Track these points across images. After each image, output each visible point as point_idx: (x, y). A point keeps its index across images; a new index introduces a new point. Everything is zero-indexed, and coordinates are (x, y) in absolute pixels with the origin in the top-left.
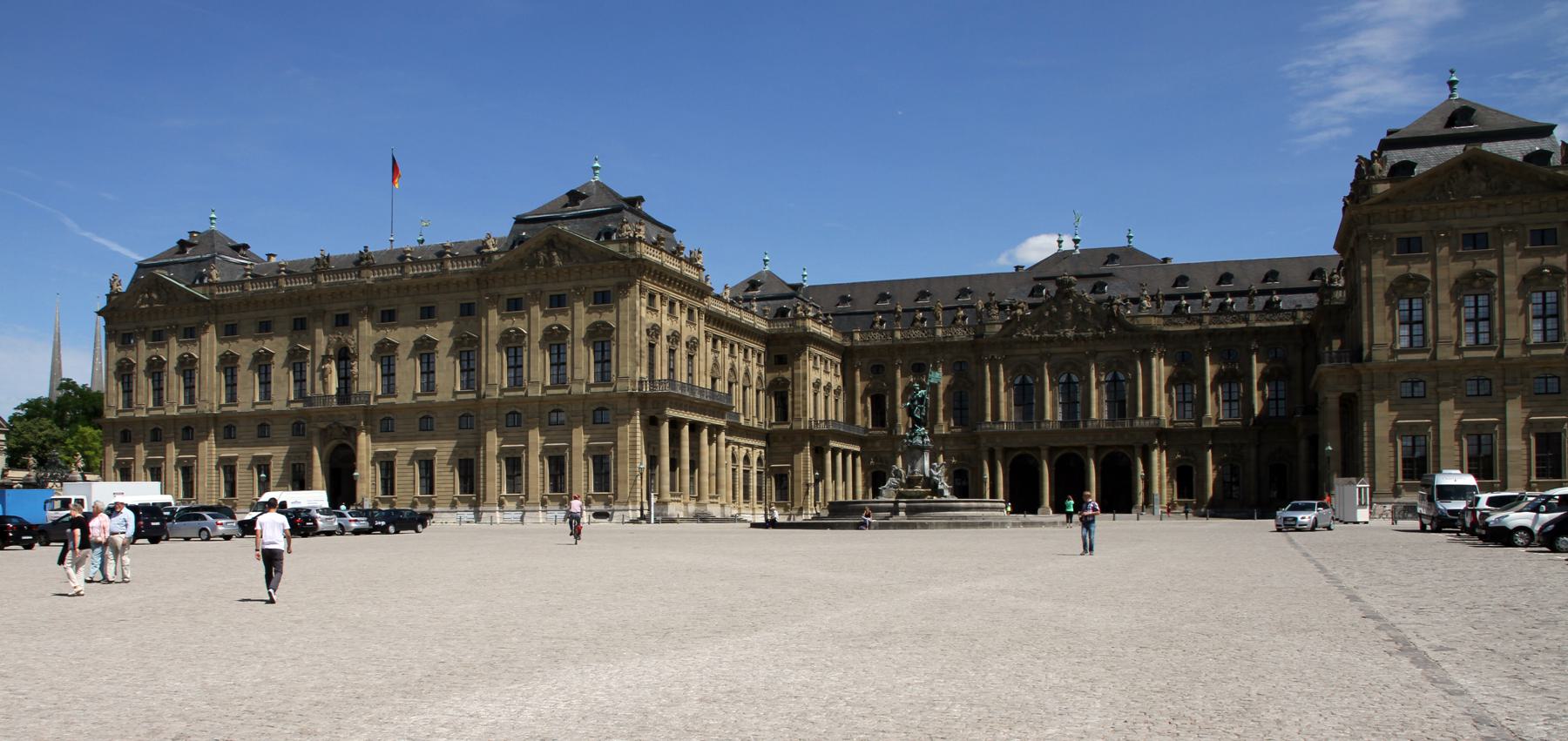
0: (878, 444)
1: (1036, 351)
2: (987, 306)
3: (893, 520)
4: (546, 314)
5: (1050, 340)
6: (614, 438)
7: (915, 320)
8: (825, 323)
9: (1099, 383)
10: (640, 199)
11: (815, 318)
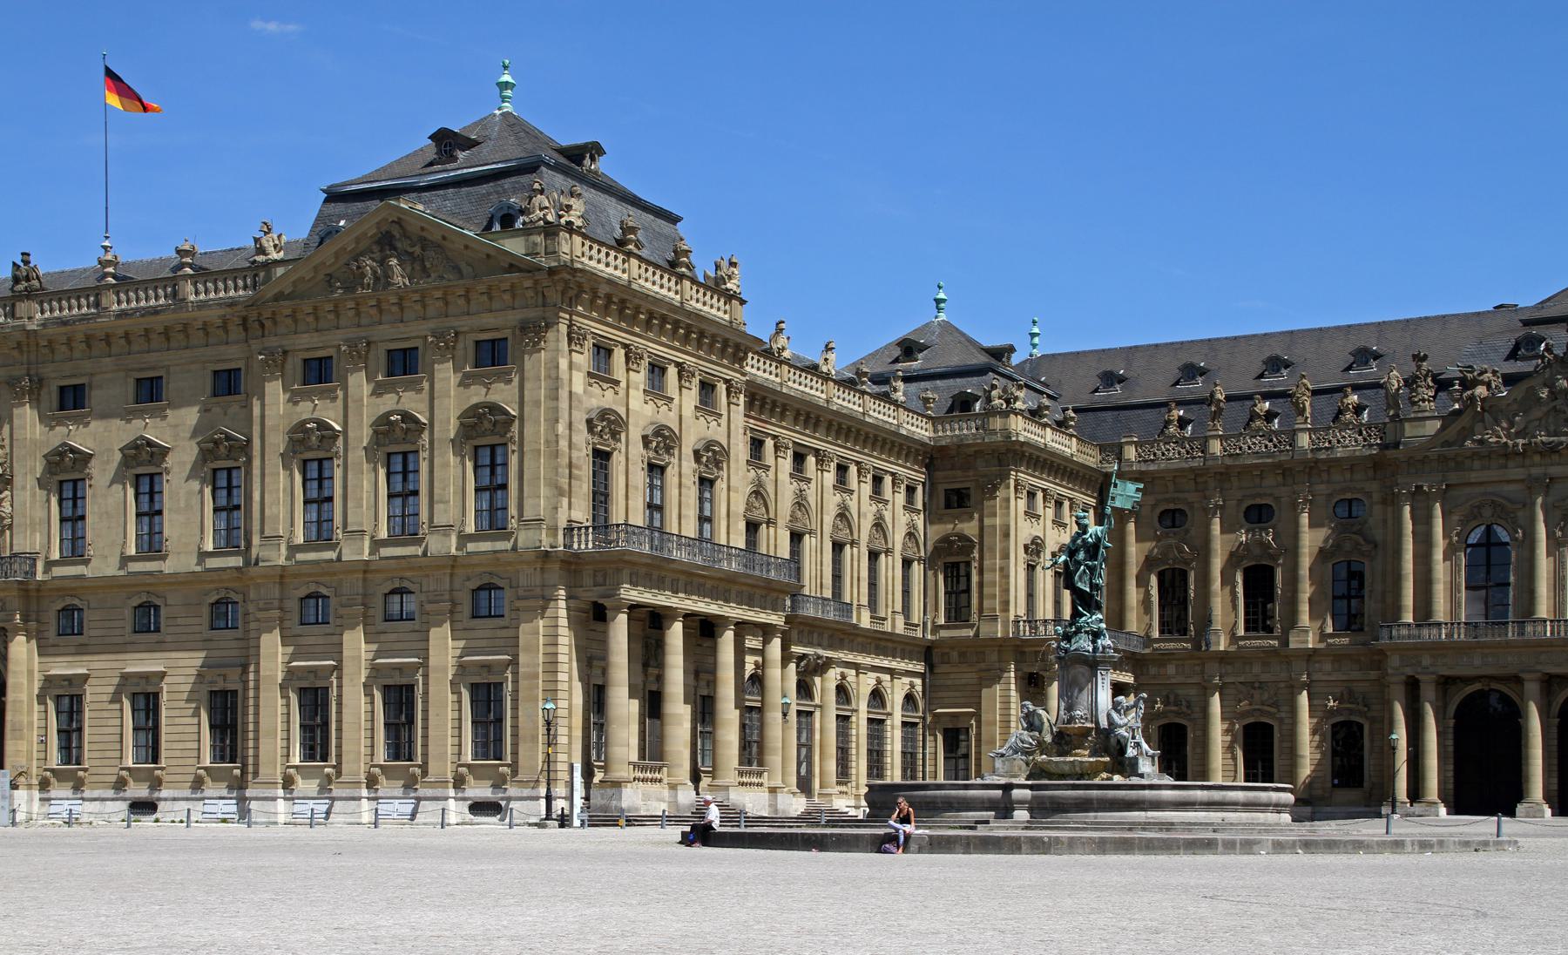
0: (1171, 669)
1: (1515, 472)
2: (1410, 382)
3: (999, 829)
4: (377, 392)
6: (513, 646)
7: (1253, 416)
8: (1061, 425)
10: (595, 150)
11: (1034, 414)
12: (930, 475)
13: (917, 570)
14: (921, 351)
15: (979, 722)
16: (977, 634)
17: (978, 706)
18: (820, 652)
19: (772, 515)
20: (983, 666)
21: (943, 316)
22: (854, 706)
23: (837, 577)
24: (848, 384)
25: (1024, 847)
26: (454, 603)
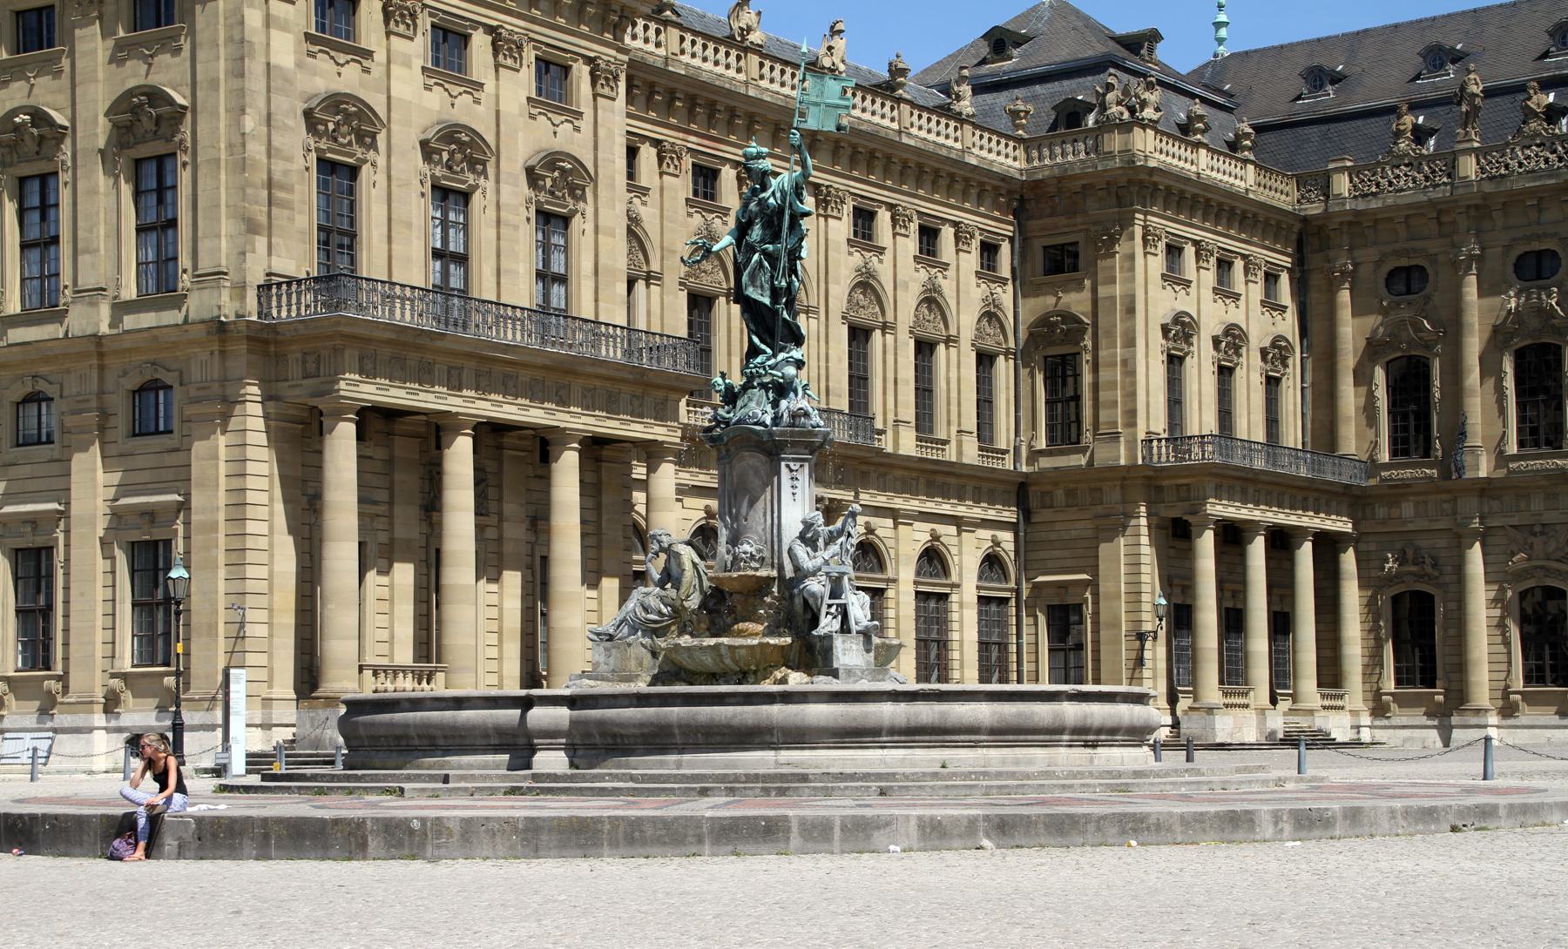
0: (1407, 509)
6: (181, 479)
12: (1021, 227)
13: (1003, 369)
14: (1018, 45)
15: (1096, 595)
16: (1091, 463)
17: (1094, 570)
19: (890, 317)
20: (1100, 509)
22: (890, 574)
23: (859, 380)
24: (887, 89)
25: (373, 844)
26: (104, 415)
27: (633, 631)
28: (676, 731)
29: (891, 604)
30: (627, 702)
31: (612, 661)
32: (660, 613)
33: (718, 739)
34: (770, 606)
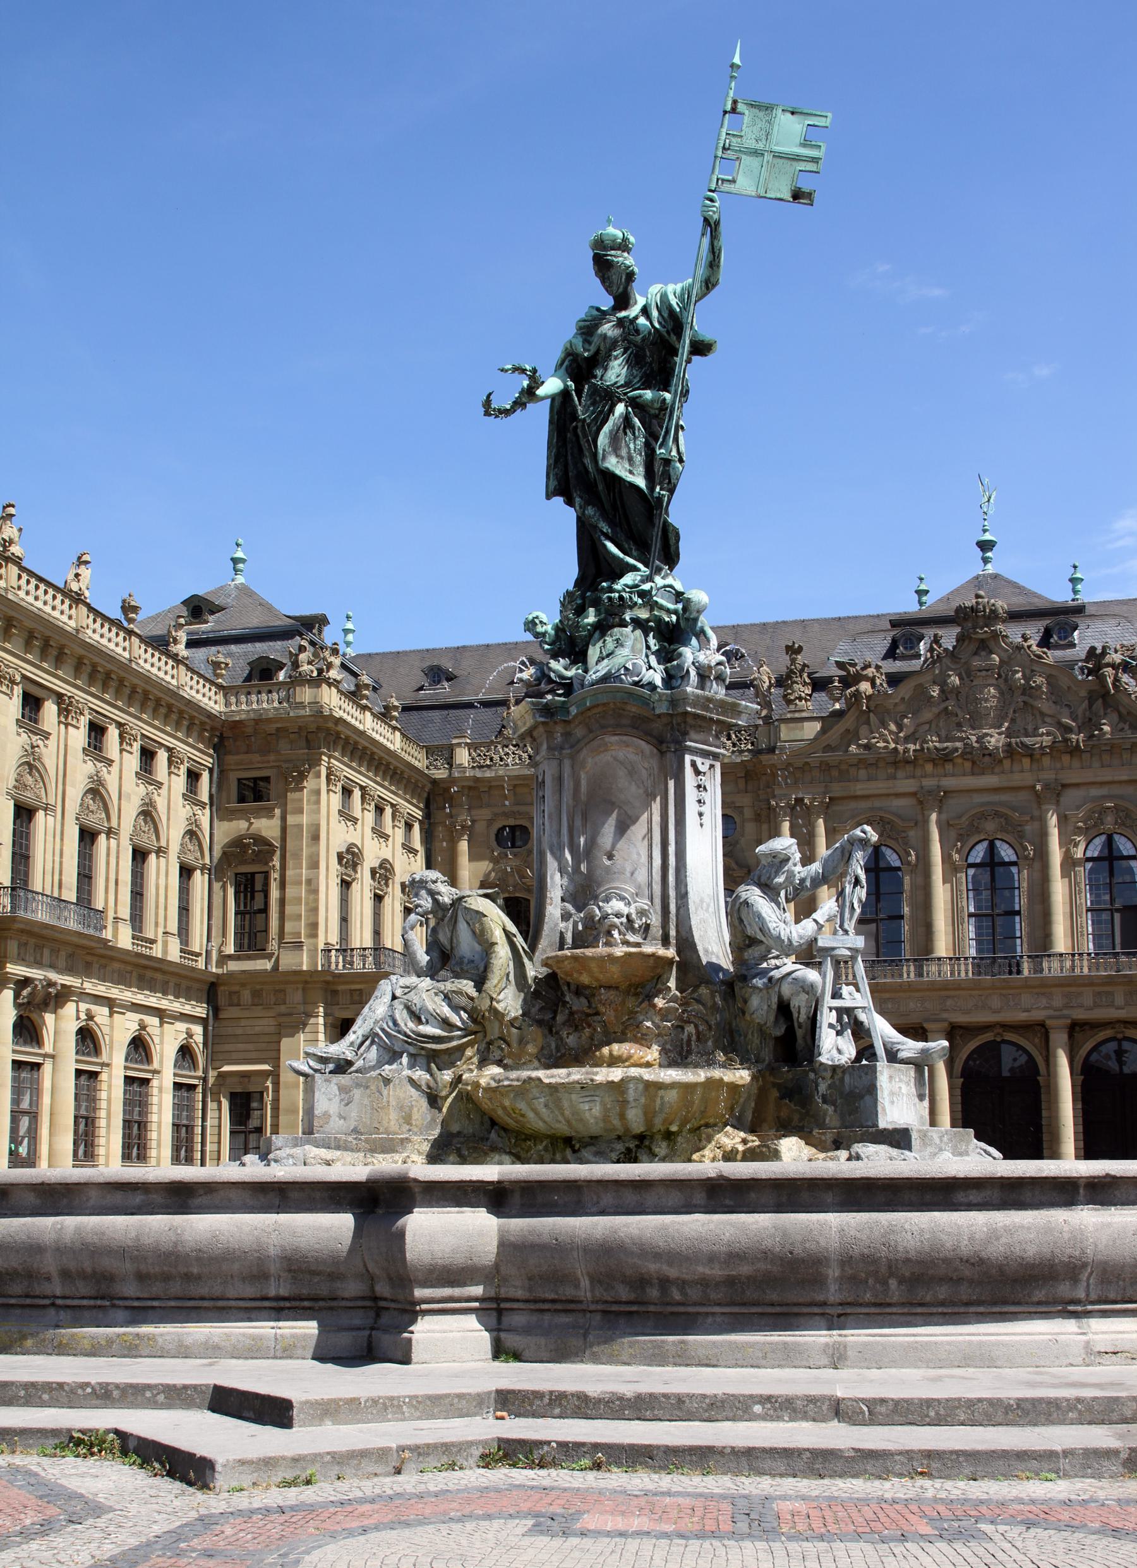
1: (907, 785)
5: (944, 758)
8: (384, 716)
9: (1069, 863)
12: (220, 761)
13: (199, 880)
14: (212, 613)
15: (276, 1084)
16: (276, 967)
17: (276, 1061)
18: (53, 976)
20: (283, 1009)
21: (240, 579)
22: (104, 1058)
23: (85, 877)
27: (393, 1056)
28: (833, 1272)
29: (104, 1086)
30: (675, 1198)
31: (353, 1112)
32: (446, 1023)
33: (943, 1292)
34: (664, 1014)
